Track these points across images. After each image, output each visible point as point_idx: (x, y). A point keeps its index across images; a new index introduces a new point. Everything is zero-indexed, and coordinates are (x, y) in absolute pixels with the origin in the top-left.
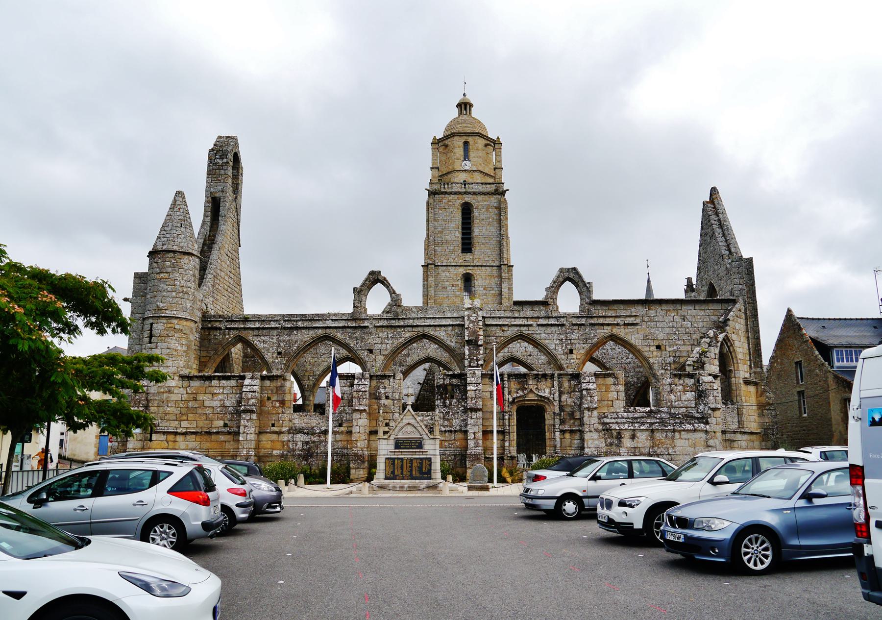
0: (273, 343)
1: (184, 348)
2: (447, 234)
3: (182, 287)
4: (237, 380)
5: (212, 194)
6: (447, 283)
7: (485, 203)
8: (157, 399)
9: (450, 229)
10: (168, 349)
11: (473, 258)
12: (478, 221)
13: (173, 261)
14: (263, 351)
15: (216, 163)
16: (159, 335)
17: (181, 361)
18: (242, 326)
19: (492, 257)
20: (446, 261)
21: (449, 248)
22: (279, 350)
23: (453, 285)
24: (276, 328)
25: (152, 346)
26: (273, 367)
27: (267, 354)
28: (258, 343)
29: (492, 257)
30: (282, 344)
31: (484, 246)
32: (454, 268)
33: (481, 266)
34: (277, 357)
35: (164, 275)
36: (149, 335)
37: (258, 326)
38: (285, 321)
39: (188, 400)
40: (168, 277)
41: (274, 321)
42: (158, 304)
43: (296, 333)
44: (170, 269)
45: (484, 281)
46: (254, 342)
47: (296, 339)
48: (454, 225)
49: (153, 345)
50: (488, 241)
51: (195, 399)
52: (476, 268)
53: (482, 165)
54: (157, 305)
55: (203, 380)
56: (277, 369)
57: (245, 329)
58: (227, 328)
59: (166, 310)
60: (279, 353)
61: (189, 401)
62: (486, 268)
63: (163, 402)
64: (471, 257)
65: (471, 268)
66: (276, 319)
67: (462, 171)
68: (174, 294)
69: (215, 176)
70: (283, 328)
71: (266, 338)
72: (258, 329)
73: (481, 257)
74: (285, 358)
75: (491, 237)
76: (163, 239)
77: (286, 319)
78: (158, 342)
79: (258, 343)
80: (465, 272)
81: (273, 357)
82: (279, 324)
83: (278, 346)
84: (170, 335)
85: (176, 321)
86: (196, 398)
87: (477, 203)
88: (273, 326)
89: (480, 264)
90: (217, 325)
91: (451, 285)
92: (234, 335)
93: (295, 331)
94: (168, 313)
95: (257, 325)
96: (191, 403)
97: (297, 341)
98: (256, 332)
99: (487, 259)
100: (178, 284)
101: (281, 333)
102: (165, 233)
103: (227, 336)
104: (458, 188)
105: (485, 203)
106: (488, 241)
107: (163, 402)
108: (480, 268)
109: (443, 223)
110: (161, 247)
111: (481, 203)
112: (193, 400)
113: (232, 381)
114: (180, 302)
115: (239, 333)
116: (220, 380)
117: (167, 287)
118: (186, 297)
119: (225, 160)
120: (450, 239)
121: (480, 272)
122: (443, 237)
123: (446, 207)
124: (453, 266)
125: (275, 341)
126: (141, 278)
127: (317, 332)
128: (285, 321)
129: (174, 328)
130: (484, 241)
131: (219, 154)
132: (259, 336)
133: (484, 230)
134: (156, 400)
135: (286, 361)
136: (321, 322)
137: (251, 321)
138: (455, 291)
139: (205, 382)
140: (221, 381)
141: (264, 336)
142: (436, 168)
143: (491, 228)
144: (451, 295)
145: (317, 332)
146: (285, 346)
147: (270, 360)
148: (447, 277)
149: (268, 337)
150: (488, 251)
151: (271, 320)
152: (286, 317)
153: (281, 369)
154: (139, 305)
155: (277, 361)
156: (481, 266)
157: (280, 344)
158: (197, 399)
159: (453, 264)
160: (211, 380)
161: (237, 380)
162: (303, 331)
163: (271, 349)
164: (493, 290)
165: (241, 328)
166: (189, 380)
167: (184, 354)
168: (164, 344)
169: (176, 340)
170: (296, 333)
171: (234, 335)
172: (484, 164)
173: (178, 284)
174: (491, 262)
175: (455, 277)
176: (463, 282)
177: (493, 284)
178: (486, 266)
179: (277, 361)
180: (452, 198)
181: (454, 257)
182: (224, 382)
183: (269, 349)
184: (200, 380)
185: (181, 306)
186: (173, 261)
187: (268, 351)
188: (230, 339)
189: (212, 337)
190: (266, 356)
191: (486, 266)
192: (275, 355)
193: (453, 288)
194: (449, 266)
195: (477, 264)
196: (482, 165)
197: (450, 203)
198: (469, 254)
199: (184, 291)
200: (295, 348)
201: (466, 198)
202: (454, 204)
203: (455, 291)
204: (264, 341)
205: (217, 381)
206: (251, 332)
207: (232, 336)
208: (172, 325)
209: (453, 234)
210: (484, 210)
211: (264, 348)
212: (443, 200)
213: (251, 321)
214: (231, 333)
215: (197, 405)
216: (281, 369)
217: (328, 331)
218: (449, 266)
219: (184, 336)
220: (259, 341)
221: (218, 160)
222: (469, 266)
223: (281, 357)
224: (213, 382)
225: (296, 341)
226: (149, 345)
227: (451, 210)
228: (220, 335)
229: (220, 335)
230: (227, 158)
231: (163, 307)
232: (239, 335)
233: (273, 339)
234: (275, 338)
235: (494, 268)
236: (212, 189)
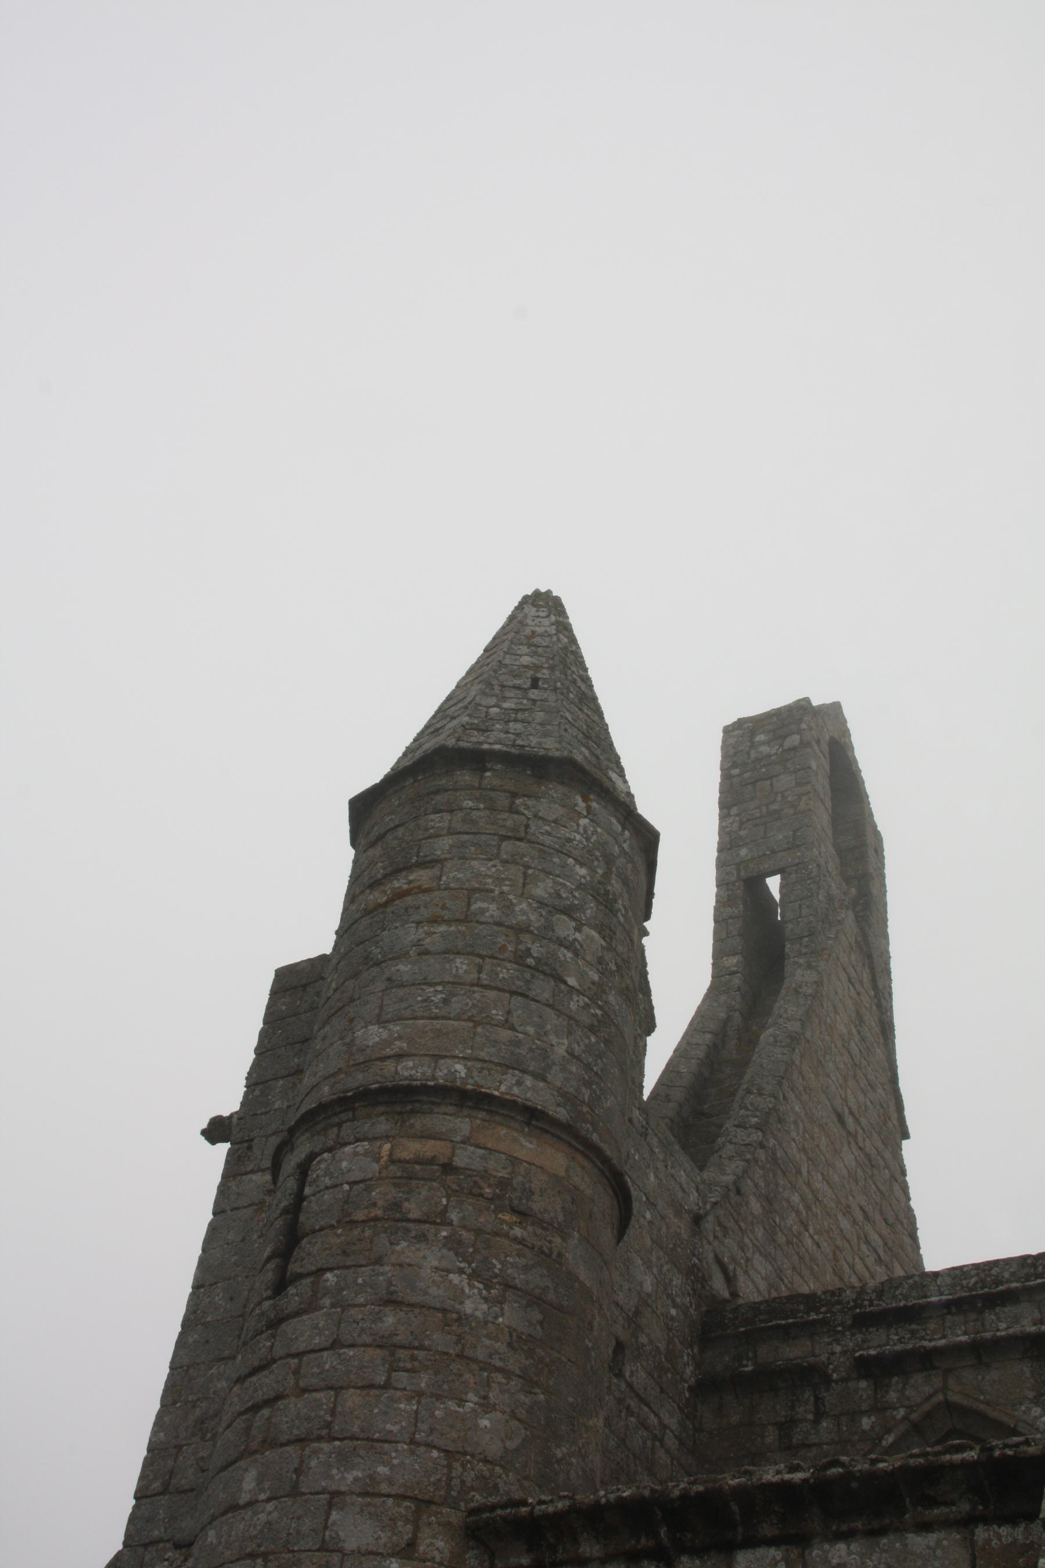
1: (511, 1316)
3: (521, 930)
17: (486, 1406)
44: (447, 842)
58: (865, 1367)
59: (400, 1056)
68: (461, 965)
84: (413, 1208)
85: (462, 1125)
90: (793, 1352)
92: (910, 1408)
94: (410, 1070)
100: (493, 910)
103: (866, 1423)
114: (498, 1014)
116: (801, 1540)
118: (542, 989)
129: (448, 1168)
165: (958, 1350)
167: (515, 1362)
169: (454, 1244)
171: (910, 1408)
173: (493, 910)
185: (505, 1034)
189: (771, 1436)
199: (528, 952)
207: (902, 1412)
208: (429, 1148)
214: (893, 1396)
219: (517, 1231)
228: (819, 1415)
229: (819, 1415)
230: (800, 732)
232: (949, 1406)
236: (743, 852)
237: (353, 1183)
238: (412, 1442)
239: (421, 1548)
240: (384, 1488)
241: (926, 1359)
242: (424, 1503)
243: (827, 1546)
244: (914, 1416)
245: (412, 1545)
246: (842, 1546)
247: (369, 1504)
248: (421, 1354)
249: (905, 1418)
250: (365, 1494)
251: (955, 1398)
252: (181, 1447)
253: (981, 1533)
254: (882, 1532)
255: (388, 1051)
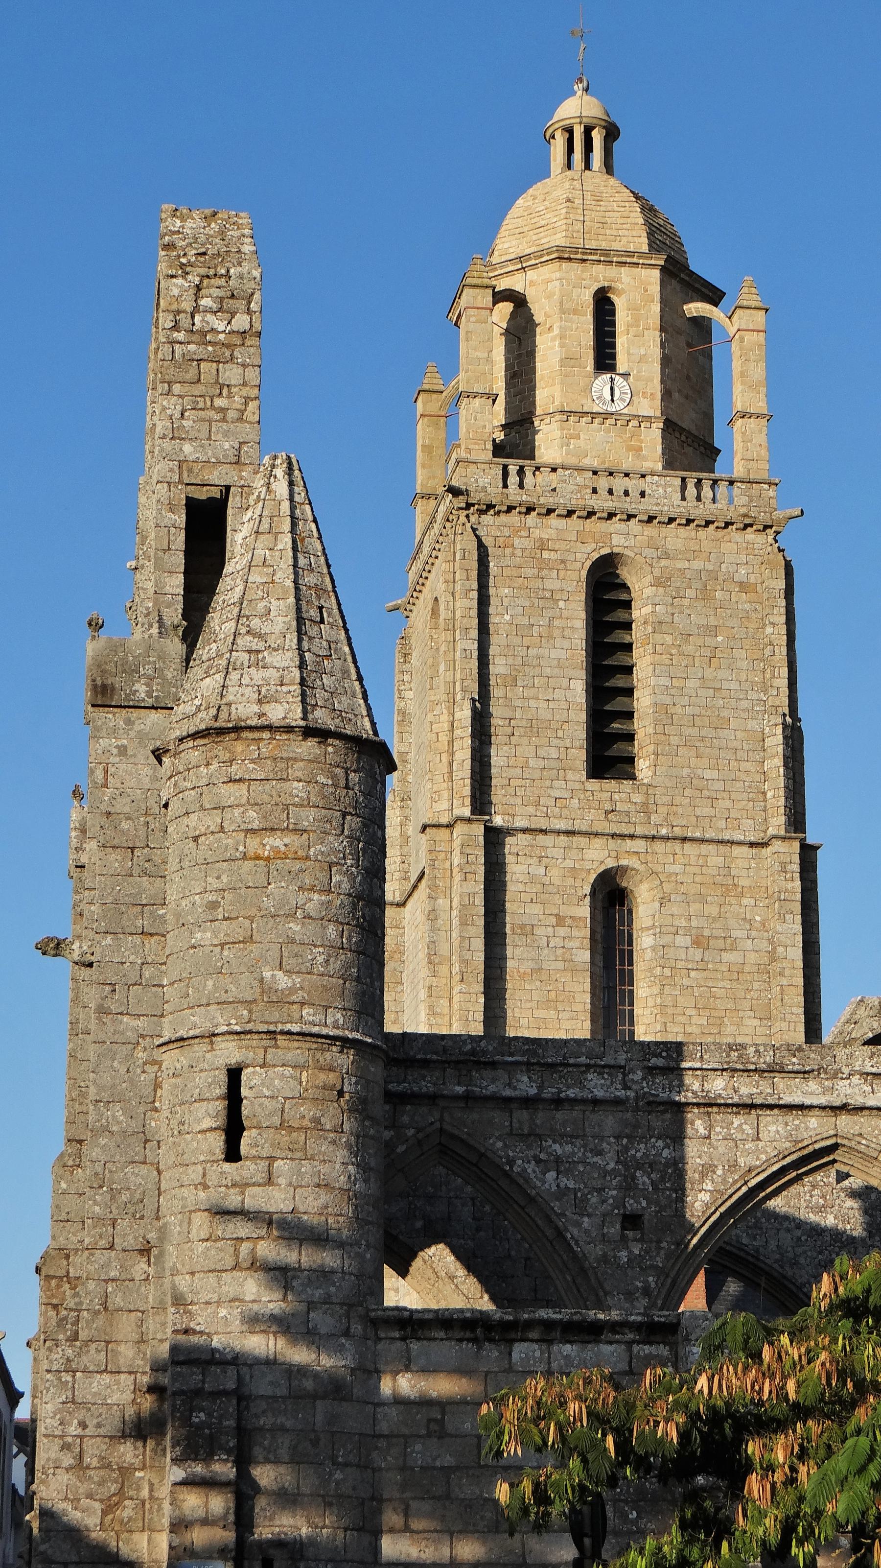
0: (605, 1173)
2: (529, 693)
4: (630, 1344)
5: (190, 471)
6: (536, 909)
7: (697, 564)
8: (289, 1424)
9: (548, 671)
10: (322, 1191)
11: (645, 804)
12: (669, 639)
13: (322, 779)
14: (556, 1206)
15: (203, 333)
16: (276, 1120)
18: (460, 1089)
19: (728, 804)
20: (531, 810)
21: (542, 753)
22: (631, 1205)
23: (560, 920)
24: (617, 1102)
25: (246, 1173)
26: (607, 1286)
27: (578, 1224)
28: (531, 1168)
29: (728, 804)
30: (643, 1179)
31: (693, 753)
32: (563, 840)
33: (684, 839)
34: (624, 1239)
35: (287, 840)
36: (221, 1121)
37: (533, 1091)
38: (651, 1071)
39: (406, 1431)
40: (300, 853)
41: (601, 1069)
42: (267, 974)
43: (702, 1131)
45: (695, 908)
46: (511, 1162)
47: (706, 1158)
48: (562, 654)
49: (246, 1169)
50: (707, 732)
51: (434, 1427)
52: (659, 846)
53: (676, 395)
54: (262, 980)
55: (475, 1340)
56: (629, 1295)
57: (468, 1098)
60: (632, 1221)
61: (407, 1440)
62: (705, 848)
63: (315, 1443)
64: (637, 798)
65: (639, 845)
66: (608, 1060)
67: (594, 415)
69: (199, 389)
70: (649, 1103)
71: (568, 1148)
72: (527, 1102)
73: (678, 800)
74: (659, 1242)
75: (725, 713)
76: (258, 675)
77: (654, 1061)
78: (278, 1153)
79: (531, 1168)
80: (610, 863)
81: (604, 1239)
82: (626, 1087)
83: (628, 1188)
86: (441, 1422)
87: (663, 563)
88: (600, 1093)
89: (678, 832)
91: (553, 920)
93: (698, 1123)
95: (526, 1086)
96: (418, 1447)
97: (712, 1168)
98: (522, 1115)
99: (707, 811)
101: (636, 1126)
102: (257, 644)
104: (581, 487)
105: (697, 564)
106: (707, 732)
107: (315, 1443)
108: (677, 846)
109: (517, 640)
110: (255, 708)
111: (680, 565)
112: (429, 1435)
113: (606, 1349)
115: (441, 1120)
116: (550, 1342)
117: (302, 898)
119: (241, 322)
120: (545, 714)
121: (677, 868)
122: (518, 703)
123: (530, 572)
124: (558, 832)
125: (612, 1165)
126: (132, 849)
127: (797, 1128)
128: (651, 1071)
130: (694, 731)
131: (216, 292)
132: (533, 1136)
133: (692, 683)
134: (283, 1429)
135: (668, 1257)
136: (812, 1085)
137: (493, 1065)
138: (569, 944)
139: (480, 1348)
140: (555, 1348)
141: (561, 1137)
142: (483, 394)
143: (721, 674)
144: (555, 965)
145: (797, 1128)
146: (656, 1189)
147: (594, 1251)
148: (532, 879)
149: (579, 1142)
150: (708, 774)
151: (588, 1067)
152: (659, 1056)
153: (646, 1291)
154: (133, 977)
155: (623, 1255)
156: (684, 839)
157: (634, 1178)
158: (450, 1428)
159: (561, 825)
160: (512, 1341)
161: (630, 1344)
162: (736, 1122)
163: (594, 1199)
164: (733, 949)
165: (456, 1098)
166: (403, 1339)
168: (306, 1167)
170: (702, 1131)
171: (419, 1130)
172: (680, 391)
174: (722, 824)
175: (570, 881)
176: (599, 905)
177: (732, 922)
178: (702, 841)
179: (623, 1255)
180: (553, 534)
181: (567, 795)
182: (567, 1349)
183: (585, 1199)
184: (460, 1340)
186: (322, 779)
187: (581, 1207)
188: (401, 1149)
190: (575, 1232)
191: (702, 841)
192: (614, 1230)
193: (562, 931)
194: (544, 832)
195: (664, 832)
196: (676, 395)
197: (546, 555)
198: (627, 784)
200: (705, 1197)
201: (616, 540)
202: (563, 562)
203: (569, 944)
204: (558, 1160)
205: (536, 1346)
206: (498, 1116)
207: (411, 1132)
209: (558, 694)
210: (690, 593)
211: (562, 1193)
212: (517, 542)
213: (493, 1065)
214: (406, 1119)
215: (448, 1460)
216: (646, 1291)
217: (845, 1122)
218: (544, 832)
220: (538, 1161)
221: (209, 317)
222: (632, 837)
223: (641, 1240)
224: (520, 1351)
225: (707, 1170)
226: (227, 1166)
227: (549, 584)
231: (292, 990)
233: (600, 1153)
234: (610, 1148)
235: (737, 851)
236: (187, 448)
237: (286, 1098)
238: (343, 1272)
239: (352, 1330)
240: (335, 1300)
241: (432, 1099)
242: (351, 1306)
243: (561, 1345)
244: (420, 1136)
245: (348, 1328)
246: (568, 1346)
247: (328, 1309)
248: (341, 1219)
249: (414, 1135)
250: (325, 1303)
251: (446, 1127)
252: (116, 1220)
253: (636, 1348)
254: (589, 1342)
255: (294, 998)
